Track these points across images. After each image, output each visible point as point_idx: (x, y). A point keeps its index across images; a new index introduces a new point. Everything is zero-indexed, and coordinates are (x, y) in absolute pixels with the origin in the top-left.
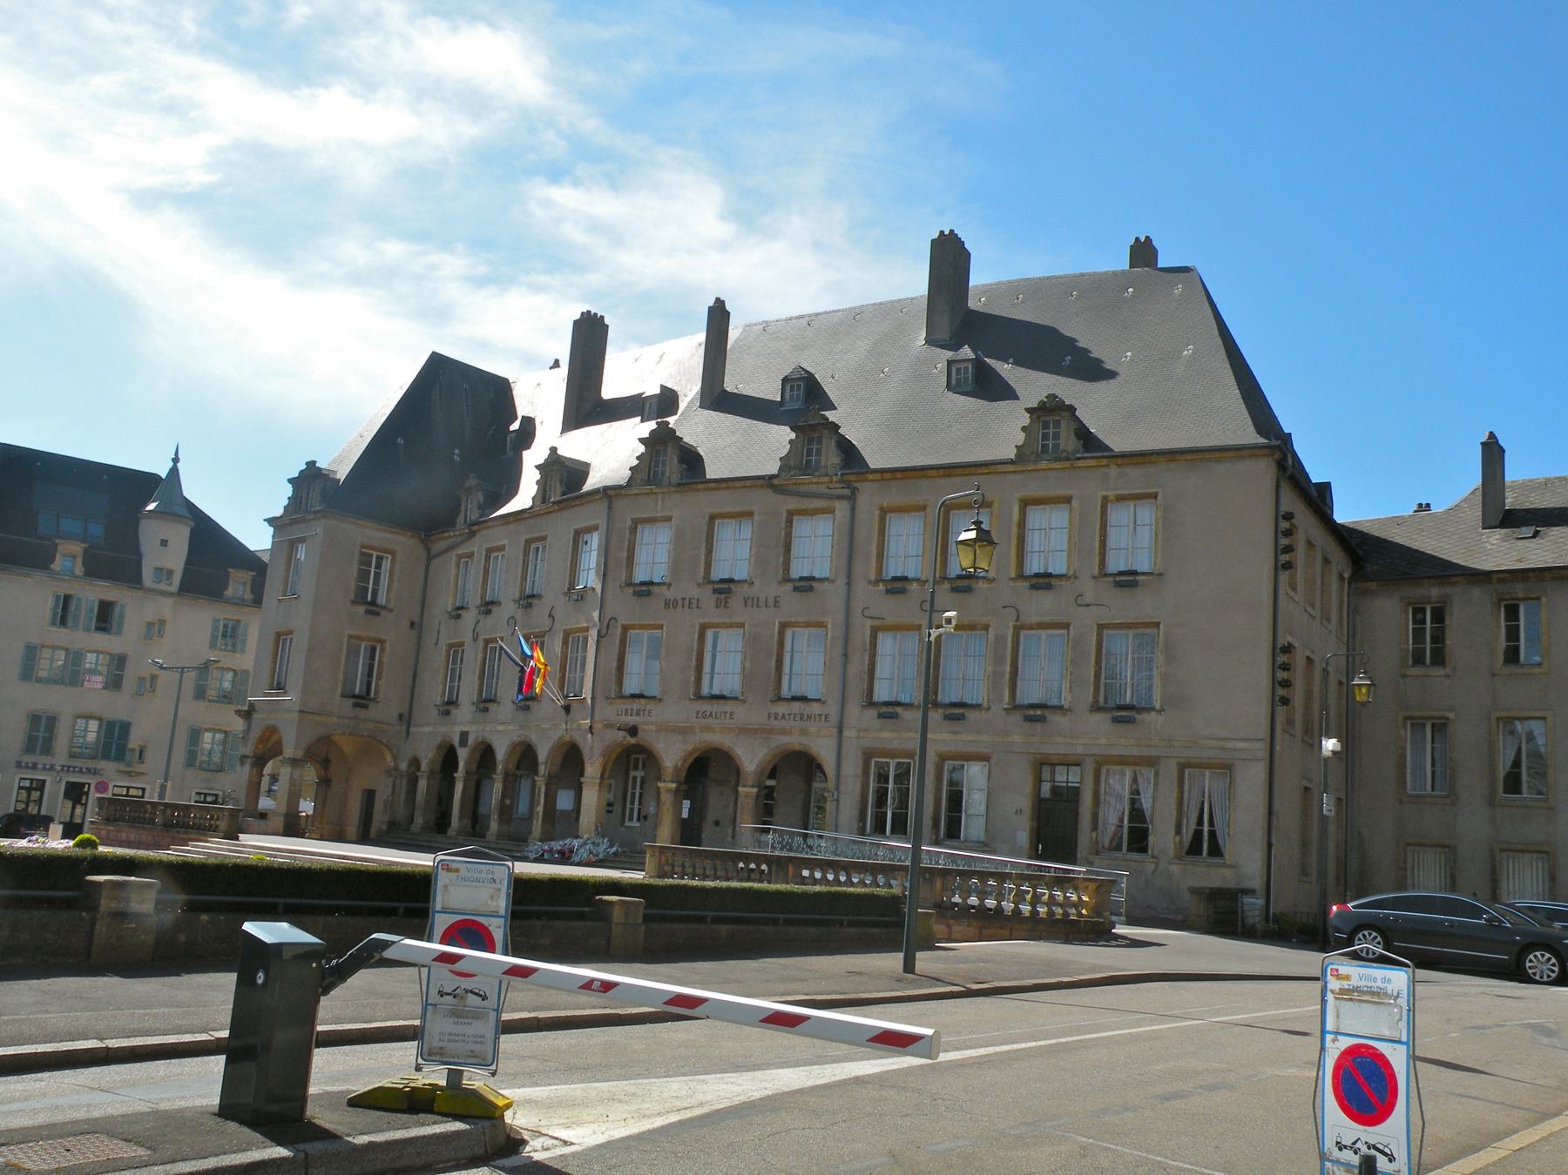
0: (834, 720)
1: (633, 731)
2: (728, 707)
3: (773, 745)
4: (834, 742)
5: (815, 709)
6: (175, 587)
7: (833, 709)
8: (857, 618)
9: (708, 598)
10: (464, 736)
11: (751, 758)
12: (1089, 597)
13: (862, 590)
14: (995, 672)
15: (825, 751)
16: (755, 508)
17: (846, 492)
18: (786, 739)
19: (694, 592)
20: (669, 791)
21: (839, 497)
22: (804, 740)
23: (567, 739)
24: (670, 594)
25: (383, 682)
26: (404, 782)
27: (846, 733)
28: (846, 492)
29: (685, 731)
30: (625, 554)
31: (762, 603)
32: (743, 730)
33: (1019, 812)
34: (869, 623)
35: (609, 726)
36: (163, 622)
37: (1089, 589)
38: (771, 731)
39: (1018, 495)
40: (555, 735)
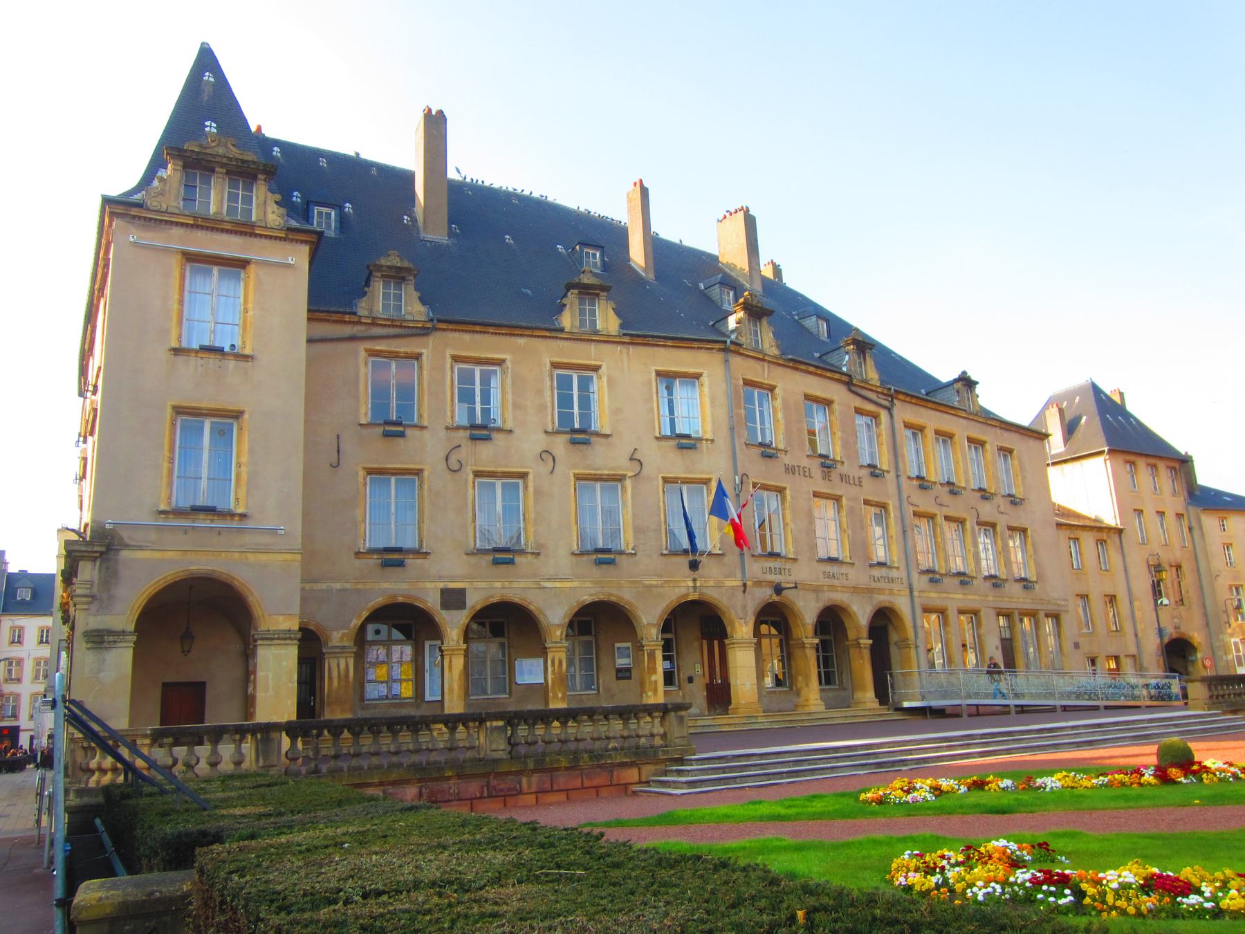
1: (778, 589)
2: (844, 569)
3: (875, 602)
4: (908, 599)
5: (894, 573)
8: (905, 504)
9: (816, 471)
15: (902, 604)
16: (835, 398)
19: (805, 462)
23: (694, 596)
24: (787, 459)
29: (817, 590)
32: (856, 590)
34: (912, 508)
35: (758, 584)
38: (870, 591)
39: (966, 434)
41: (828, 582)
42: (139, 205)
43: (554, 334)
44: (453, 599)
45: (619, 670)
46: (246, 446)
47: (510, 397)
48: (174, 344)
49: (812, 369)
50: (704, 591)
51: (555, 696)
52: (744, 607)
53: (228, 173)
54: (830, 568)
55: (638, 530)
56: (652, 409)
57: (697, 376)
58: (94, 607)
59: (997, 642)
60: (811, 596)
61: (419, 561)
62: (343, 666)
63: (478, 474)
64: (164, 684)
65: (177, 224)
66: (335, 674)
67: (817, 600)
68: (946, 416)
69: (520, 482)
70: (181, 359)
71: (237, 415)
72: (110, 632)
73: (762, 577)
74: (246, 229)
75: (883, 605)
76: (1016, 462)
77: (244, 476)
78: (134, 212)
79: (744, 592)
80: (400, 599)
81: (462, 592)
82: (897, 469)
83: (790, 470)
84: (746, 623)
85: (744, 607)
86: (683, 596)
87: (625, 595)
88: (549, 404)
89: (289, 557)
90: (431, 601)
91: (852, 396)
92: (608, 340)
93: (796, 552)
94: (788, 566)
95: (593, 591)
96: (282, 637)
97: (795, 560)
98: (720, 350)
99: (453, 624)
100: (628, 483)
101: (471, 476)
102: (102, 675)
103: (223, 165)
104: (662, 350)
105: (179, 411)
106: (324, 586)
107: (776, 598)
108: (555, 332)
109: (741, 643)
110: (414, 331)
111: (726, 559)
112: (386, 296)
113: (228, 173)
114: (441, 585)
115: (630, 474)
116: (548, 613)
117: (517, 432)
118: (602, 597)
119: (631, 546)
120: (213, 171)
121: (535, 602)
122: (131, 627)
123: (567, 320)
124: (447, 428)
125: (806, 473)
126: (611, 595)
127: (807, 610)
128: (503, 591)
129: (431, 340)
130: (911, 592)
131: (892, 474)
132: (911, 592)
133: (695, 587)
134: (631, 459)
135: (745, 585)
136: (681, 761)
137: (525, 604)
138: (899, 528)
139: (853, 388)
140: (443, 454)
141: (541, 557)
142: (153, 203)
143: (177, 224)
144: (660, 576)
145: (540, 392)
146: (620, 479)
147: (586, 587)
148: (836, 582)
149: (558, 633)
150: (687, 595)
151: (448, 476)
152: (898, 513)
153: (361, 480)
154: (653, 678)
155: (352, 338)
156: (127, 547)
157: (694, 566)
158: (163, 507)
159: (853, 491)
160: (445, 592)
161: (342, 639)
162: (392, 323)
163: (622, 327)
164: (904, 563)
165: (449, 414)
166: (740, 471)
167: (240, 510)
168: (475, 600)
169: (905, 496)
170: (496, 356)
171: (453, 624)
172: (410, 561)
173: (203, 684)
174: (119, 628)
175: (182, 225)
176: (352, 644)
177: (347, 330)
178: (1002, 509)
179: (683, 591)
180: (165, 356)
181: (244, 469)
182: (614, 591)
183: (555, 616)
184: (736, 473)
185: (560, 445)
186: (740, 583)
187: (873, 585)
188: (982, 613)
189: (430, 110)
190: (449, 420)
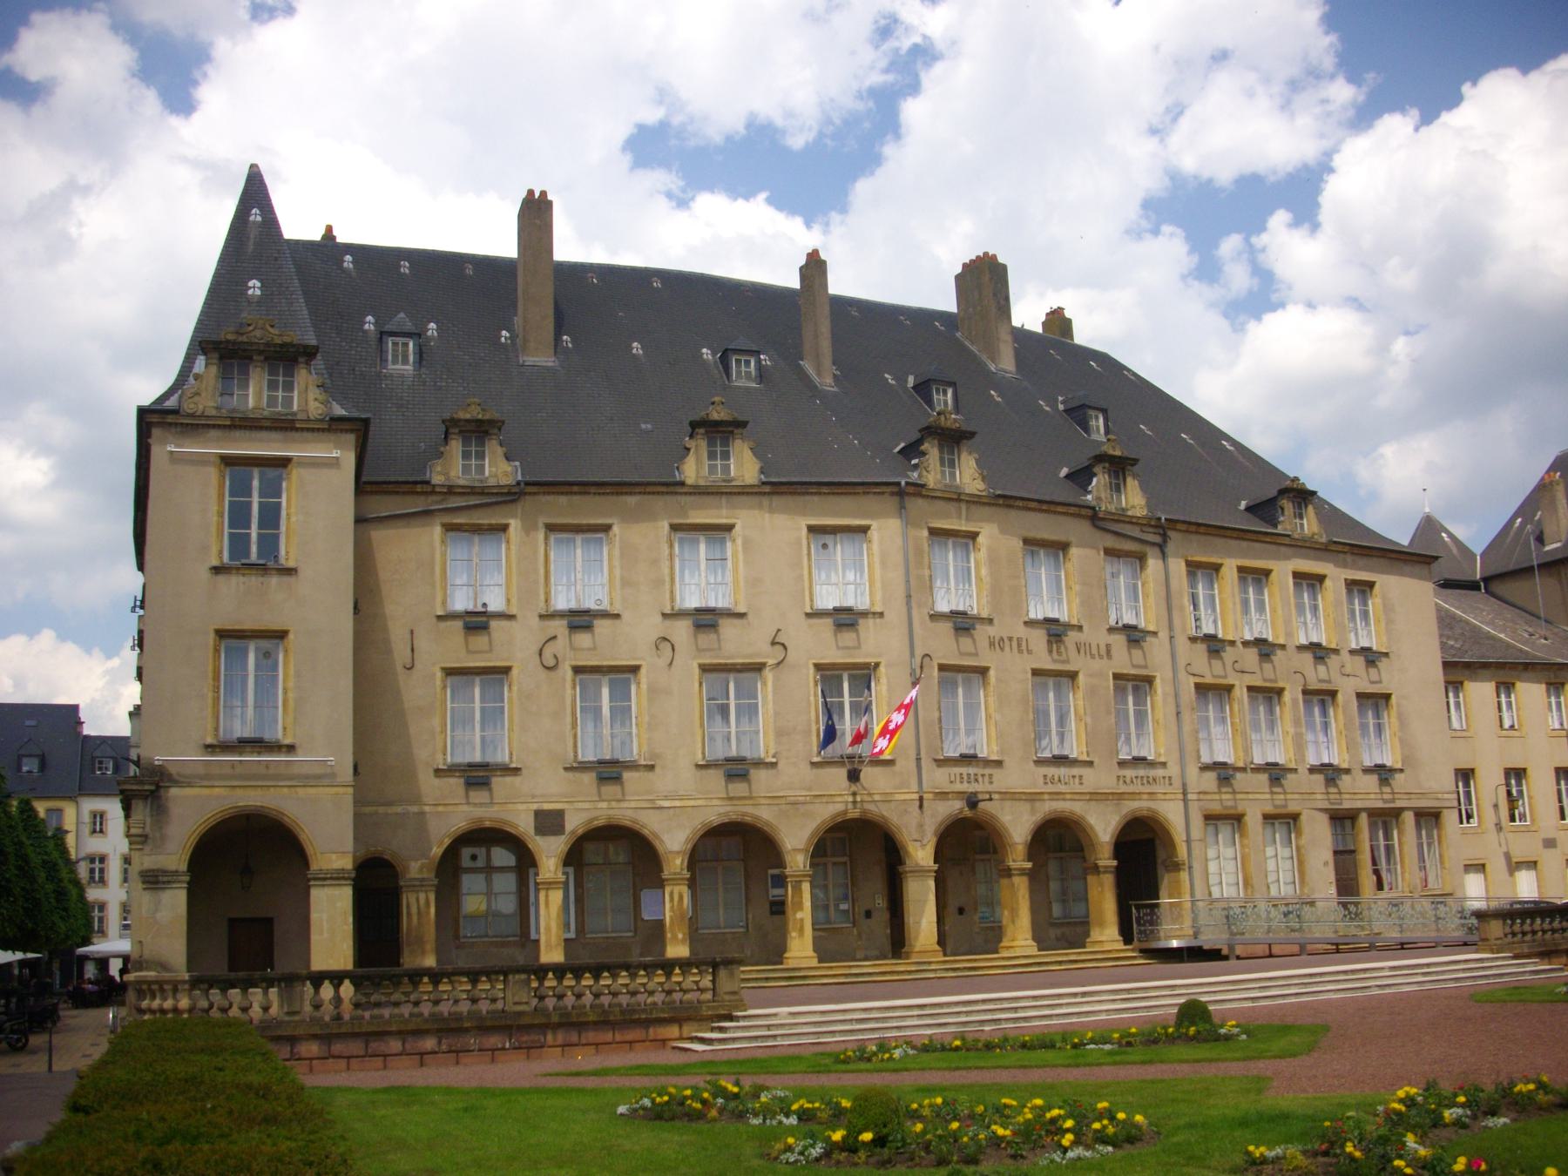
0: (1177, 783)
1: (972, 801)
2: (1076, 771)
3: (1124, 811)
5: (1160, 772)
7: (1173, 770)
8: (1182, 675)
13: (1182, 643)
15: (1172, 813)
16: (1073, 539)
17: (1158, 539)
18: (1135, 805)
20: (1022, 872)
21: (1154, 544)
23: (854, 814)
27: (1190, 796)
28: (1158, 539)
29: (1033, 798)
31: (1094, 651)
32: (1095, 796)
34: (1192, 680)
35: (942, 795)
37: (1345, 655)
38: (1119, 797)
40: (825, 813)
41: (1050, 788)
42: (175, 412)
43: (671, 489)
44: (549, 822)
45: (773, 904)
46: (292, 672)
47: (618, 572)
48: (215, 563)
49: (1033, 505)
50: (867, 806)
51: (675, 937)
52: (921, 826)
53: (266, 359)
54: (1052, 771)
55: (780, 733)
56: (801, 577)
57: (864, 530)
58: (147, 849)
59: (1328, 856)
60: (1024, 807)
61: (508, 779)
62: (422, 902)
63: (578, 670)
64: (233, 922)
65: (214, 426)
66: (414, 910)
67: (1033, 811)
68: (1257, 545)
69: (631, 676)
70: (221, 578)
71: (281, 635)
72: (165, 872)
74: (285, 425)
75: (1138, 814)
76: (1378, 600)
77: (291, 703)
78: (170, 419)
79: (921, 806)
80: (488, 824)
81: (560, 814)
82: (1171, 628)
83: (996, 644)
84: (923, 846)
85: (921, 826)
86: (838, 814)
87: (765, 814)
88: (667, 579)
89: (341, 790)
90: (523, 824)
91: (1098, 534)
92: (744, 492)
93: (1002, 752)
94: (987, 771)
95: (722, 810)
96: (335, 878)
97: (999, 763)
98: (893, 494)
99: (550, 854)
100: (768, 674)
101: (569, 673)
102: (158, 915)
103: (260, 352)
104: (816, 498)
105: (222, 634)
106: (399, 809)
107: (967, 813)
108: (674, 487)
109: (921, 872)
110: (500, 499)
111: (897, 768)
112: (466, 455)
113: (266, 359)
114: (535, 807)
115: (771, 662)
116: (665, 838)
117: (626, 616)
118: (734, 817)
119: (772, 752)
120: (251, 358)
121: (650, 823)
122: (184, 867)
123: (693, 470)
124: (541, 617)
125: (1021, 646)
126: (744, 814)
127: (1018, 826)
128: (611, 812)
129: (519, 507)
130: (1185, 793)
132: (1185, 793)
133: (854, 802)
134: (773, 643)
135: (921, 799)
136: (731, 1018)
137: (637, 827)
138: (1172, 709)
139: (1101, 524)
140: (535, 648)
141: (657, 769)
142: (188, 407)
143: (214, 426)
144: (810, 789)
145: (655, 562)
146: (758, 668)
147: (712, 804)
148: (1062, 788)
149: (678, 862)
150: (845, 812)
151: (543, 674)
152: (1170, 689)
153: (438, 683)
154: (799, 915)
155: (427, 513)
156: (176, 783)
157: (854, 776)
158: (210, 740)
159: (1097, 664)
160: (539, 814)
161: (421, 869)
162: (471, 491)
163: (762, 471)
164: (1176, 755)
165: (542, 597)
166: (919, 653)
167: (287, 741)
168: (575, 822)
169: (1182, 662)
170: (600, 521)
171: (550, 854)
172: (498, 782)
173: (268, 922)
174: (173, 867)
175: (219, 426)
176: (432, 875)
177: (419, 504)
178: (1348, 670)
179: (840, 807)
180: (204, 574)
181: (291, 695)
182: (750, 810)
183: (674, 841)
184: (912, 654)
185: (682, 631)
186: (916, 796)
187: (1123, 789)
188: (1303, 818)
189: (531, 192)
190: (542, 604)
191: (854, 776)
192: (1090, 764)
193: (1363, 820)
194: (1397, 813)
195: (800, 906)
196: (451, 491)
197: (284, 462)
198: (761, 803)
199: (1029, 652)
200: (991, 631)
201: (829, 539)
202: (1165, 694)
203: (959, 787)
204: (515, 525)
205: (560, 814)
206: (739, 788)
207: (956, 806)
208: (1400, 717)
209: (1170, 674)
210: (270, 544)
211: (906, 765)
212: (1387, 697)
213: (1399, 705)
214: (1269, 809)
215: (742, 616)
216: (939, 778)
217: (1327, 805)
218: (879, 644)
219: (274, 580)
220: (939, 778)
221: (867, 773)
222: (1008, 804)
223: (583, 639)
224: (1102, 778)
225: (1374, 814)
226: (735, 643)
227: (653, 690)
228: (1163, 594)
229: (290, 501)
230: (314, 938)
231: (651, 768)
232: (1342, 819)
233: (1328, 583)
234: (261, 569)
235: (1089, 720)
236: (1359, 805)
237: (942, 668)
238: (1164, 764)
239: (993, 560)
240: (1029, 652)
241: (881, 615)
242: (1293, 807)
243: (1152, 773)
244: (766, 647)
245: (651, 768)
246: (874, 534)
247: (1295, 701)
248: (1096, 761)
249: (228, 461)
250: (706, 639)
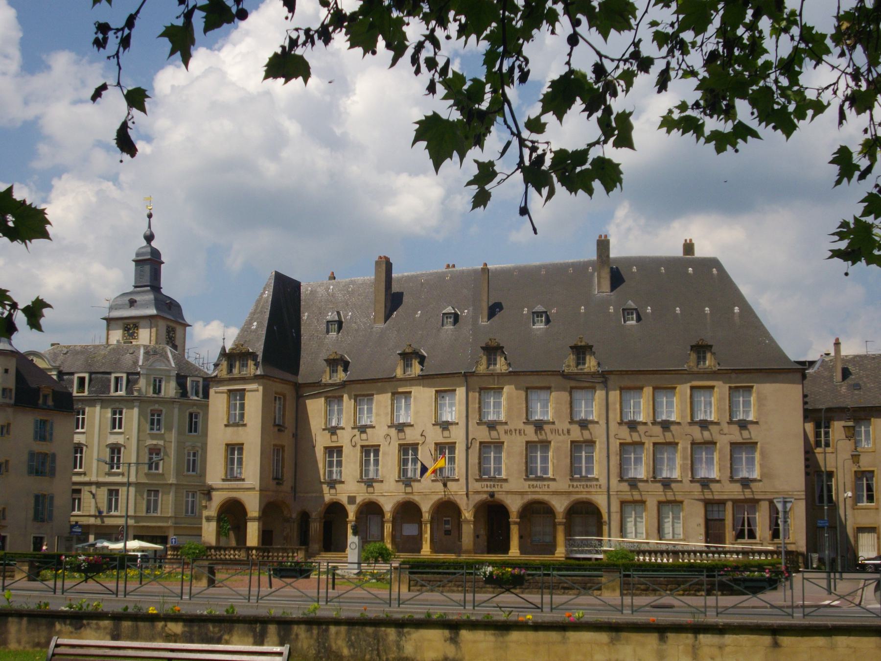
0: (604, 488)
1: (492, 495)
2: (546, 483)
4: (605, 497)
5: (595, 483)
6: (12, 401)
7: (603, 481)
8: (612, 440)
10: (352, 500)
11: (560, 506)
12: (726, 431)
13: (613, 425)
14: (684, 464)
15: (601, 501)
16: (553, 385)
19: (521, 426)
20: (515, 523)
22: (588, 496)
23: (446, 499)
25: (285, 470)
26: (296, 525)
28: (602, 379)
29: (522, 493)
30: (477, 406)
31: (560, 432)
33: (699, 525)
34: (618, 442)
35: (478, 492)
36: (9, 425)
37: (725, 426)
38: (570, 493)
40: (436, 498)
44: (352, 500)
45: (445, 531)
59: (701, 520)
60: (518, 497)
63: (362, 447)
73: (480, 489)
74: (244, 380)
81: (355, 497)
85: (467, 504)
87: (416, 498)
90: (344, 500)
96: (253, 519)
109: (468, 522)
121: (382, 501)
131: (603, 422)
145: (386, 407)
146: (418, 444)
148: (537, 489)
151: (351, 448)
157: (445, 485)
159: (562, 438)
160: (349, 497)
168: (359, 500)
169: (612, 434)
173: (272, 531)
180: (223, 426)
183: (388, 507)
185: (393, 432)
187: (571, 489)
191: (445, 485)
192: (554, 480)
193: (729, 505)
194: (757, 501)
195: (426, 532)
196: (326, 385)
197: (244, 390)
198: (457, 491)
199: (525, 435)
200: (506, 427)
201: (443, 394)
202: (600, 448)
203: (485, 489)
204: (346, 397)
205: (355, 497)
206: (409, 490)
207: (485, 496)
208: (763, 454)
209: (605, 439)
210: (242, 416)
211: (463, 481)
212: (756, 443)
213: (762, 448)
214: (663, 498)
215: (412, 426)
216: (478, 486)
217: (702, 497)
218: (457, 435)
219: (240, 428)
220: (478, 486)
221: (449, 484)
222: (509, 496)
223: (364, 436)
224: (563, 484)
225: (735, 502)
226: (411, 436)
227: (384, 454)
228: (604, 403)
229: (246, 402)
230: (248, 537)
231: (382, 481)
232: (708, 504)
233: (716, 389)
234: (237, 425)
235: (555, 461)
236: (725, 497)
237: (481, 443)
238: (597, 480)
239: (509, 398)
240: (525, 435)
241: (457, 424)
242: (679, 498)
243: (589, 483)
244: (419, 437)
245: (382, 481)
246: (457, 392)
247: (685, 449)
248: (557, 478)
249: (230, 391)
250: (401, 435)
